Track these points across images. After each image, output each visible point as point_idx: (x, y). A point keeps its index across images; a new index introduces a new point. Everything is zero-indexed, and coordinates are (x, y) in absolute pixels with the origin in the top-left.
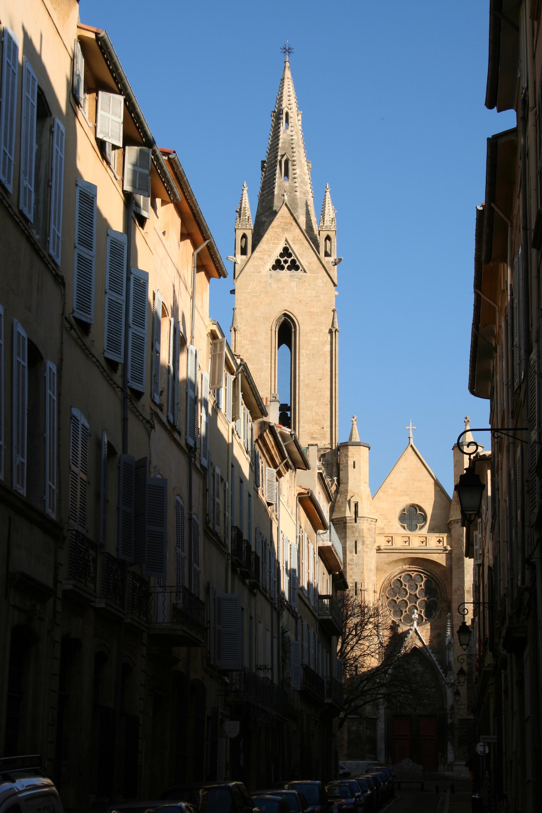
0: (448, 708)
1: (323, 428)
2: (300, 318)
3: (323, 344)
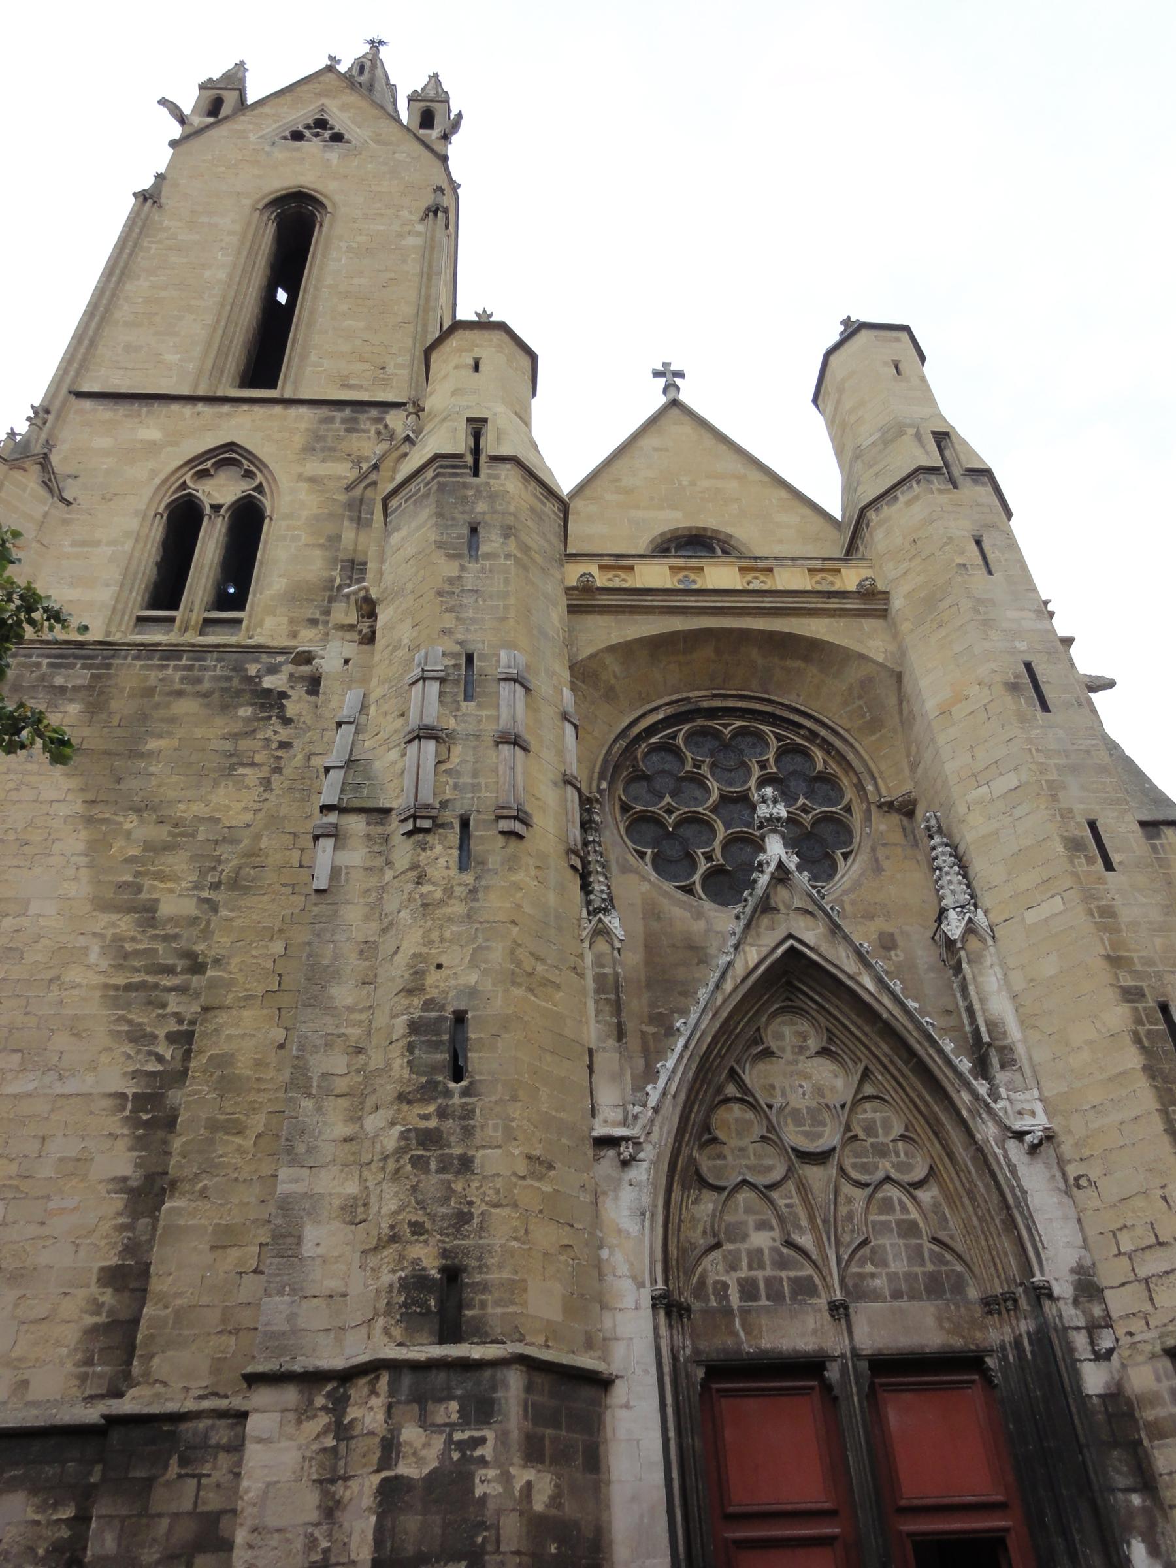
0: (1063, 1288)
1: (383, 368)
2: (337, 198)
3: (400, 235)
